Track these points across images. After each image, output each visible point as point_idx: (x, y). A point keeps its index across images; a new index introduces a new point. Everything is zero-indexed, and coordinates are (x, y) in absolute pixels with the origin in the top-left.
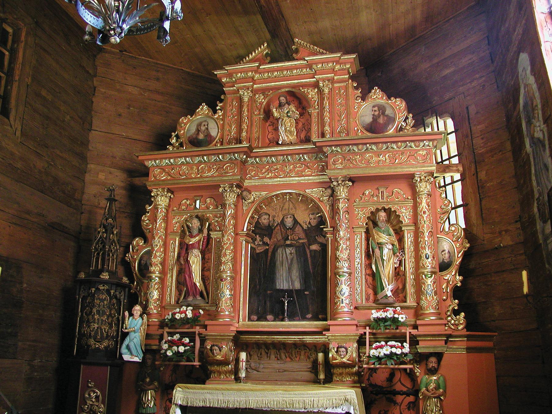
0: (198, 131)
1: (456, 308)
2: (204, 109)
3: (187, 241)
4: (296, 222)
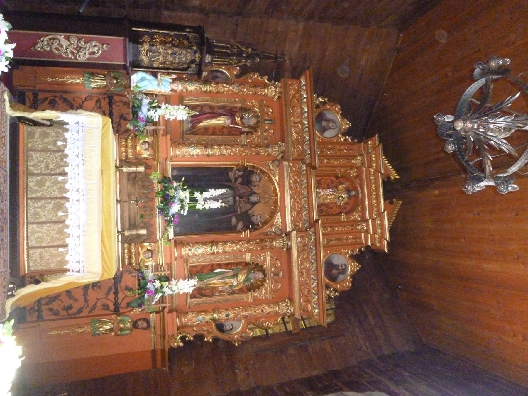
0: (328, 121)
1: (187, 339)
2: (346, 125)
3: (238, 114)
4: (254, 204)
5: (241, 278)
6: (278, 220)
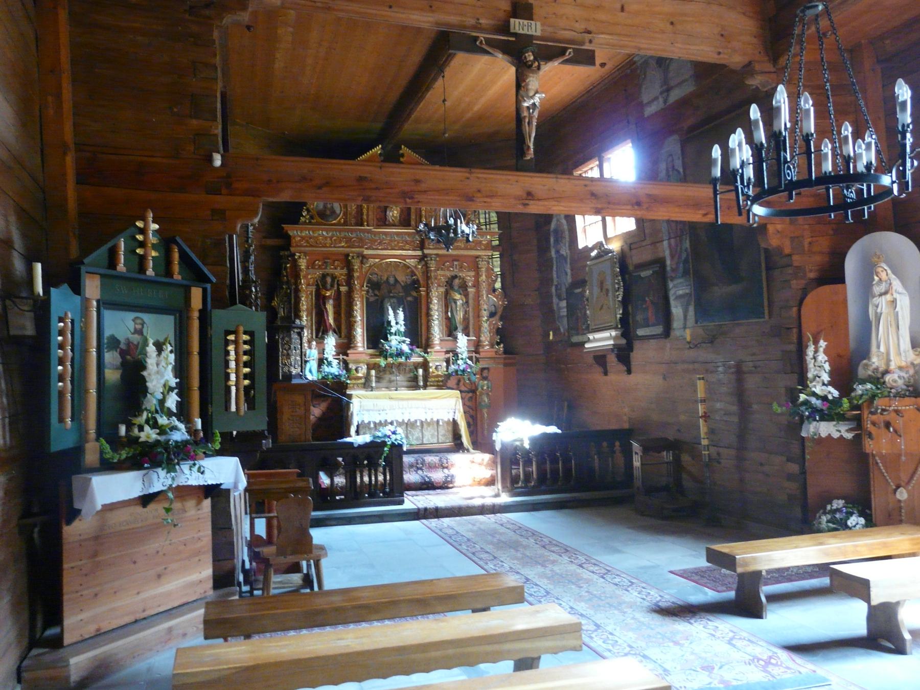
4: (396, 281)
6: (412, 262)
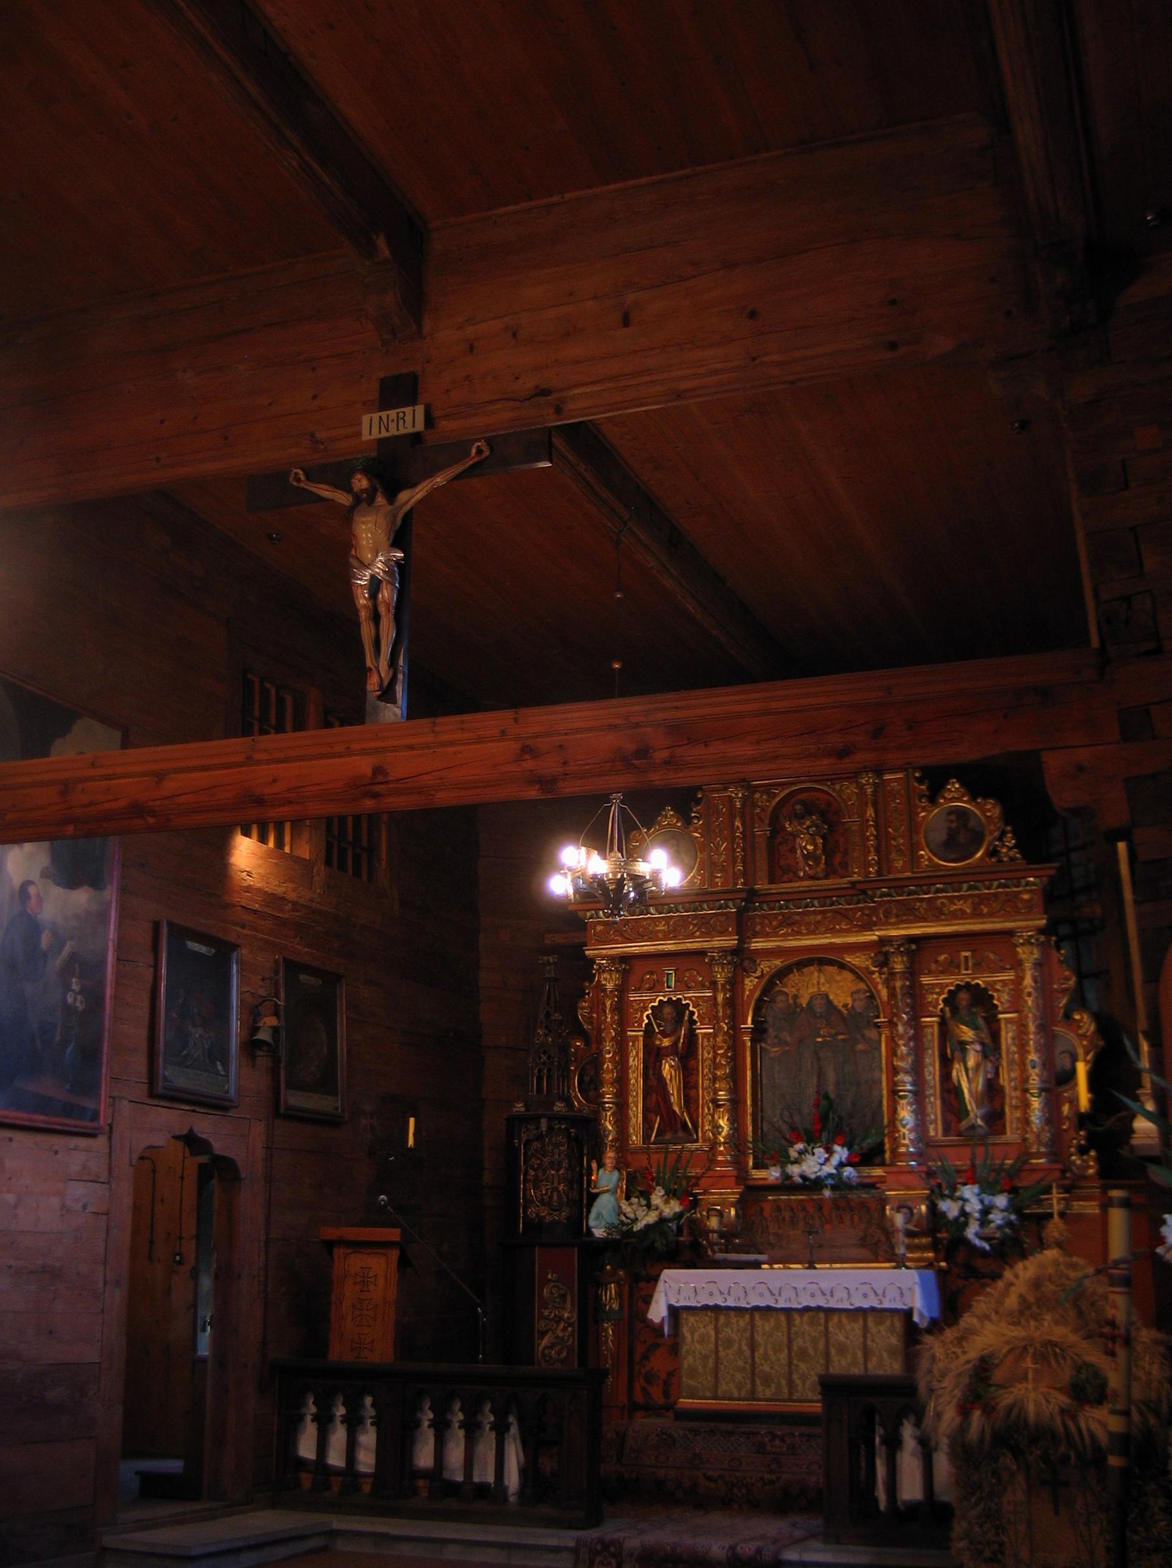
5: (967, 1033)
